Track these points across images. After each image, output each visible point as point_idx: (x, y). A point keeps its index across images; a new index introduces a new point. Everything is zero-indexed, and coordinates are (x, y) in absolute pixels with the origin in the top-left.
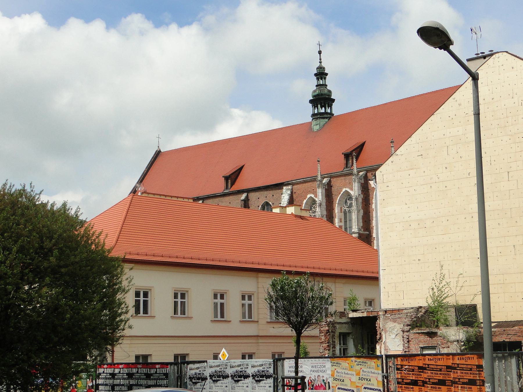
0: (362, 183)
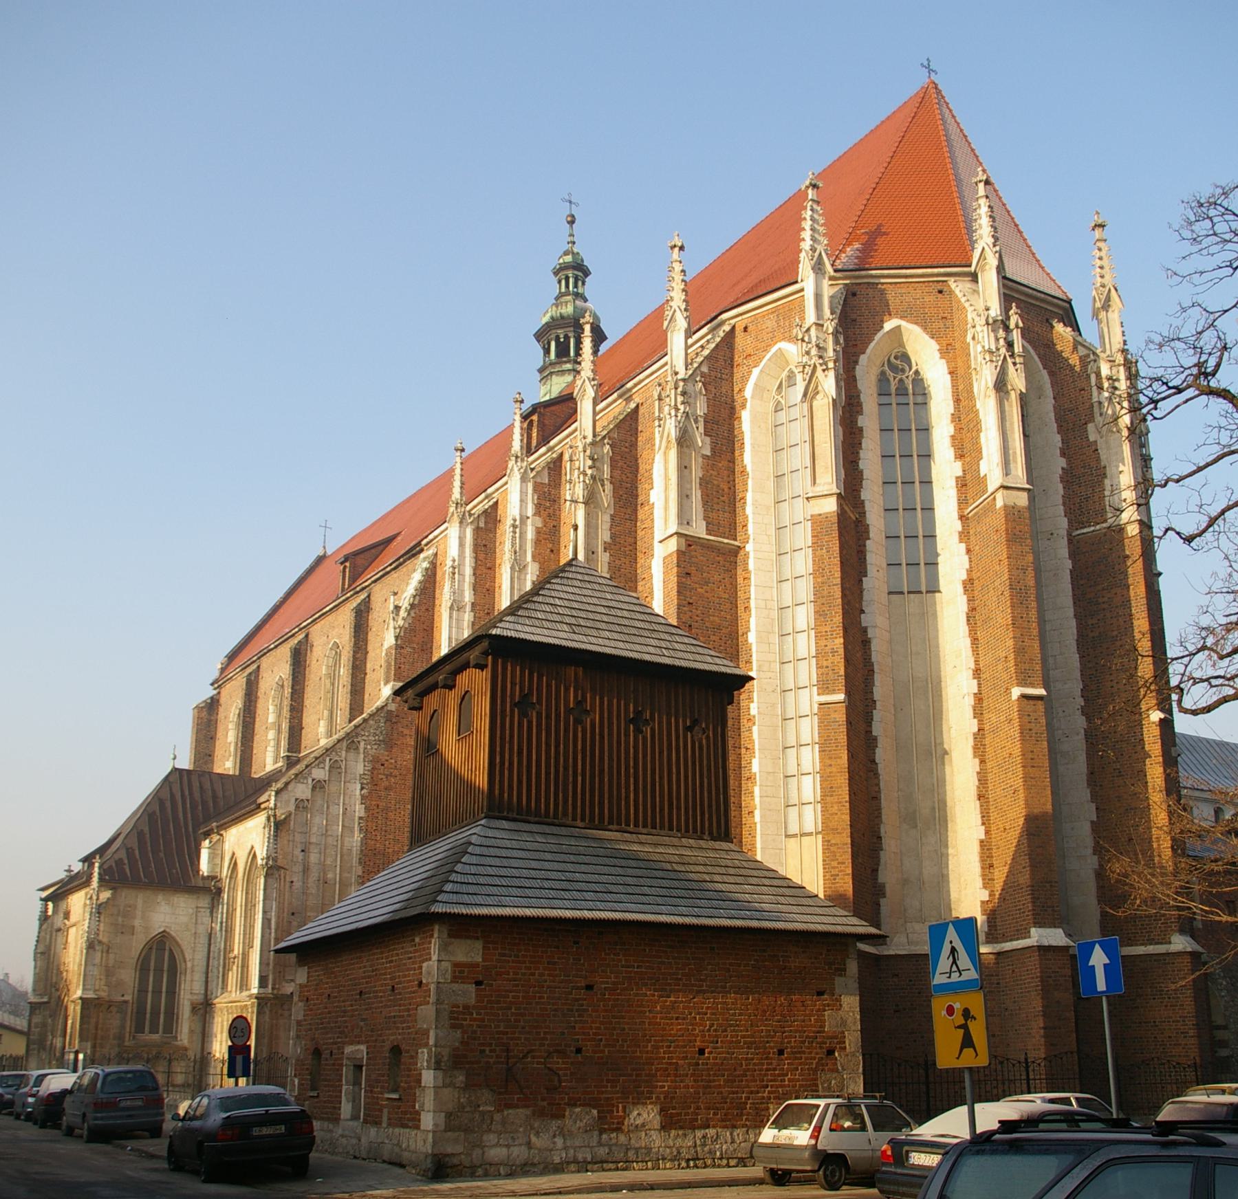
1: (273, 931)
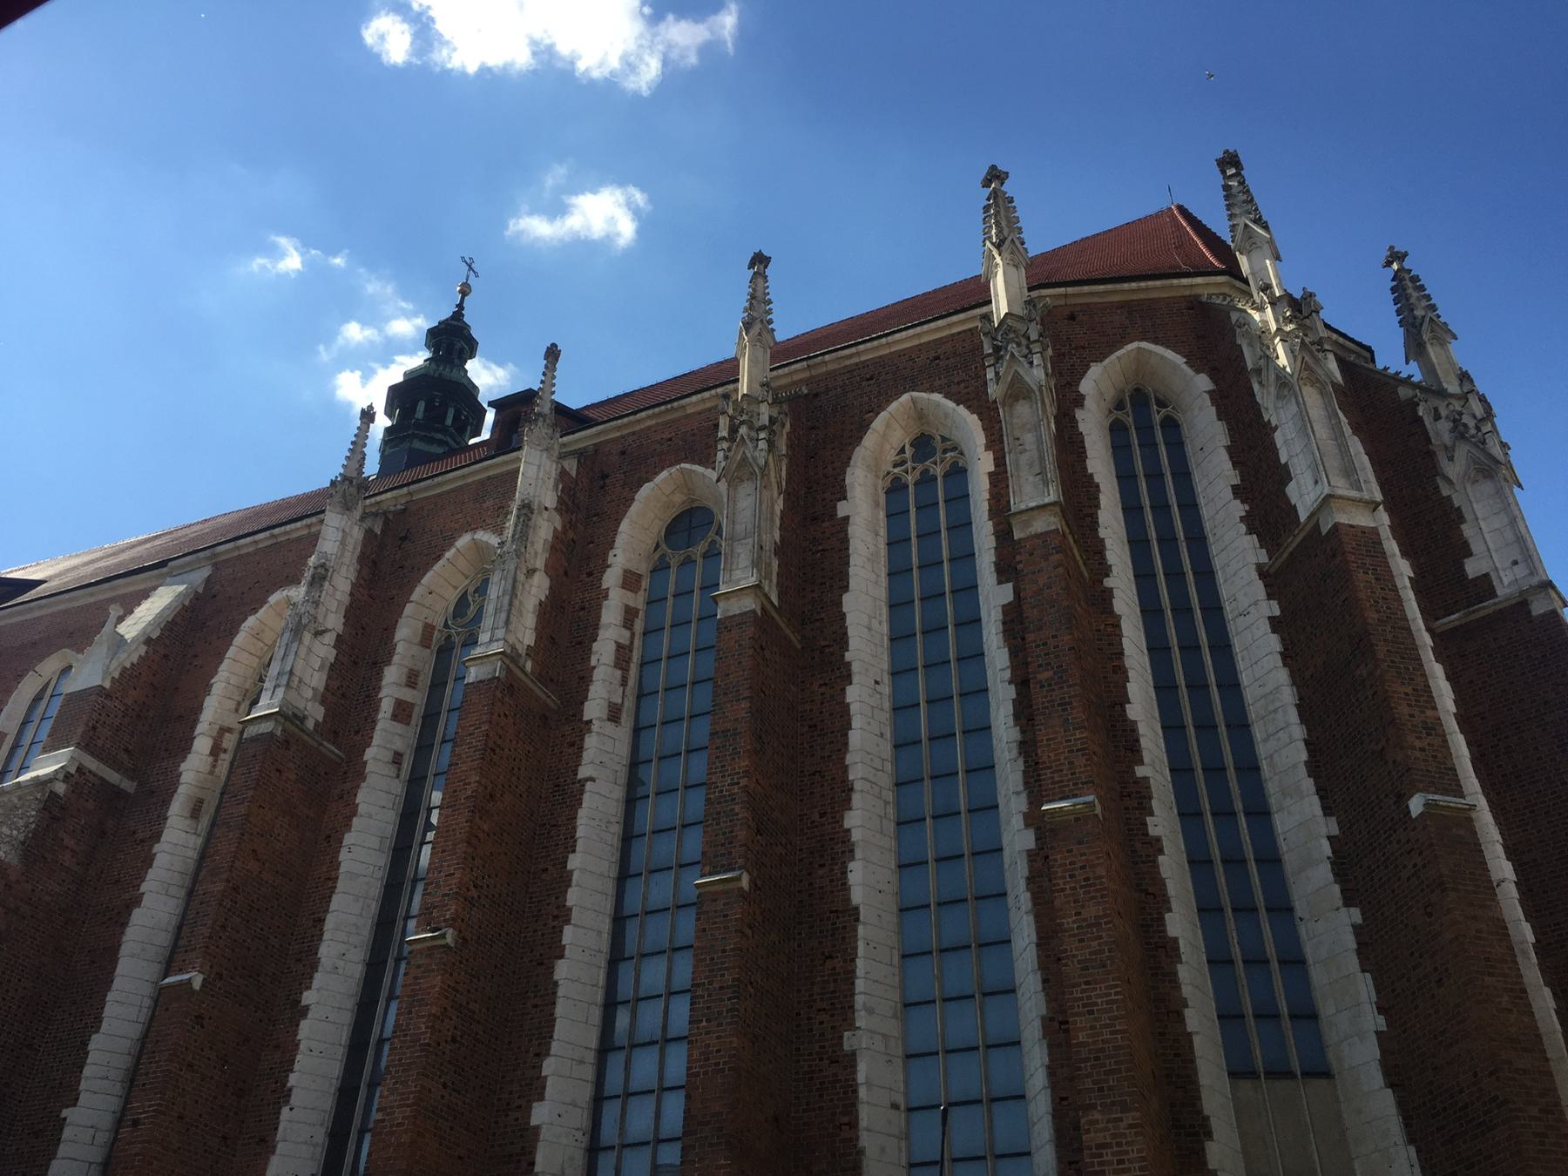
0: (563, 474)
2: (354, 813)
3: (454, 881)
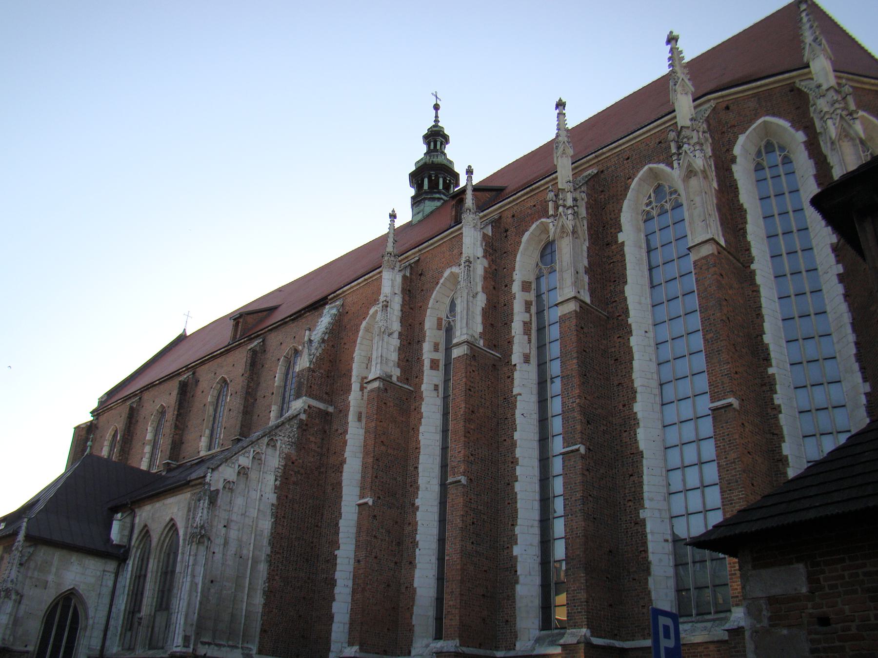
0: (485, 236)
1: (199, 594)
2: (422, 417)
3: (461, 455)
